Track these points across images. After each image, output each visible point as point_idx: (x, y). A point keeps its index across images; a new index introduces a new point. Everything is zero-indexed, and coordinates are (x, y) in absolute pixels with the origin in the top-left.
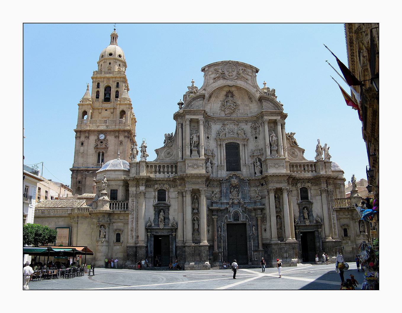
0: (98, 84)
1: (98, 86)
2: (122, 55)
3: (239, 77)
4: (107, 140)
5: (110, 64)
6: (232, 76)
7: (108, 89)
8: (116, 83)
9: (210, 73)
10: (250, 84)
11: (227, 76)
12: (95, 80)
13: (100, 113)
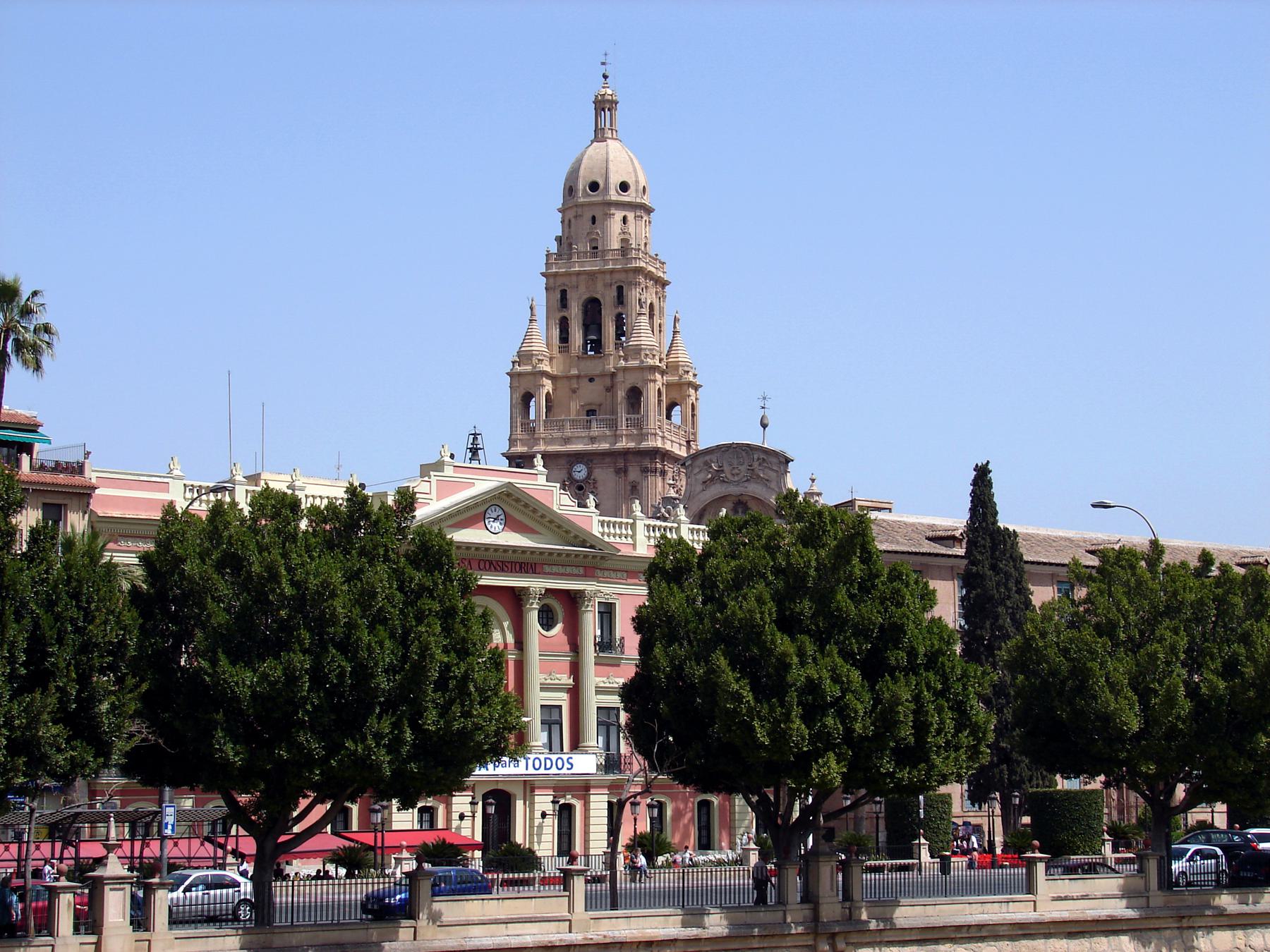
0: (564, 293)
1: (564, 303)
2: (631, 182)
3: (753, 477)
4: (595, 482)
5: (594, 219)
6: (738, 474)
7: (592, 309)
8: (614, 287)
9: (697, 470)
10: (773, 489)
11: (729, 476)
12: (551, 280)
13: (574, 391)
